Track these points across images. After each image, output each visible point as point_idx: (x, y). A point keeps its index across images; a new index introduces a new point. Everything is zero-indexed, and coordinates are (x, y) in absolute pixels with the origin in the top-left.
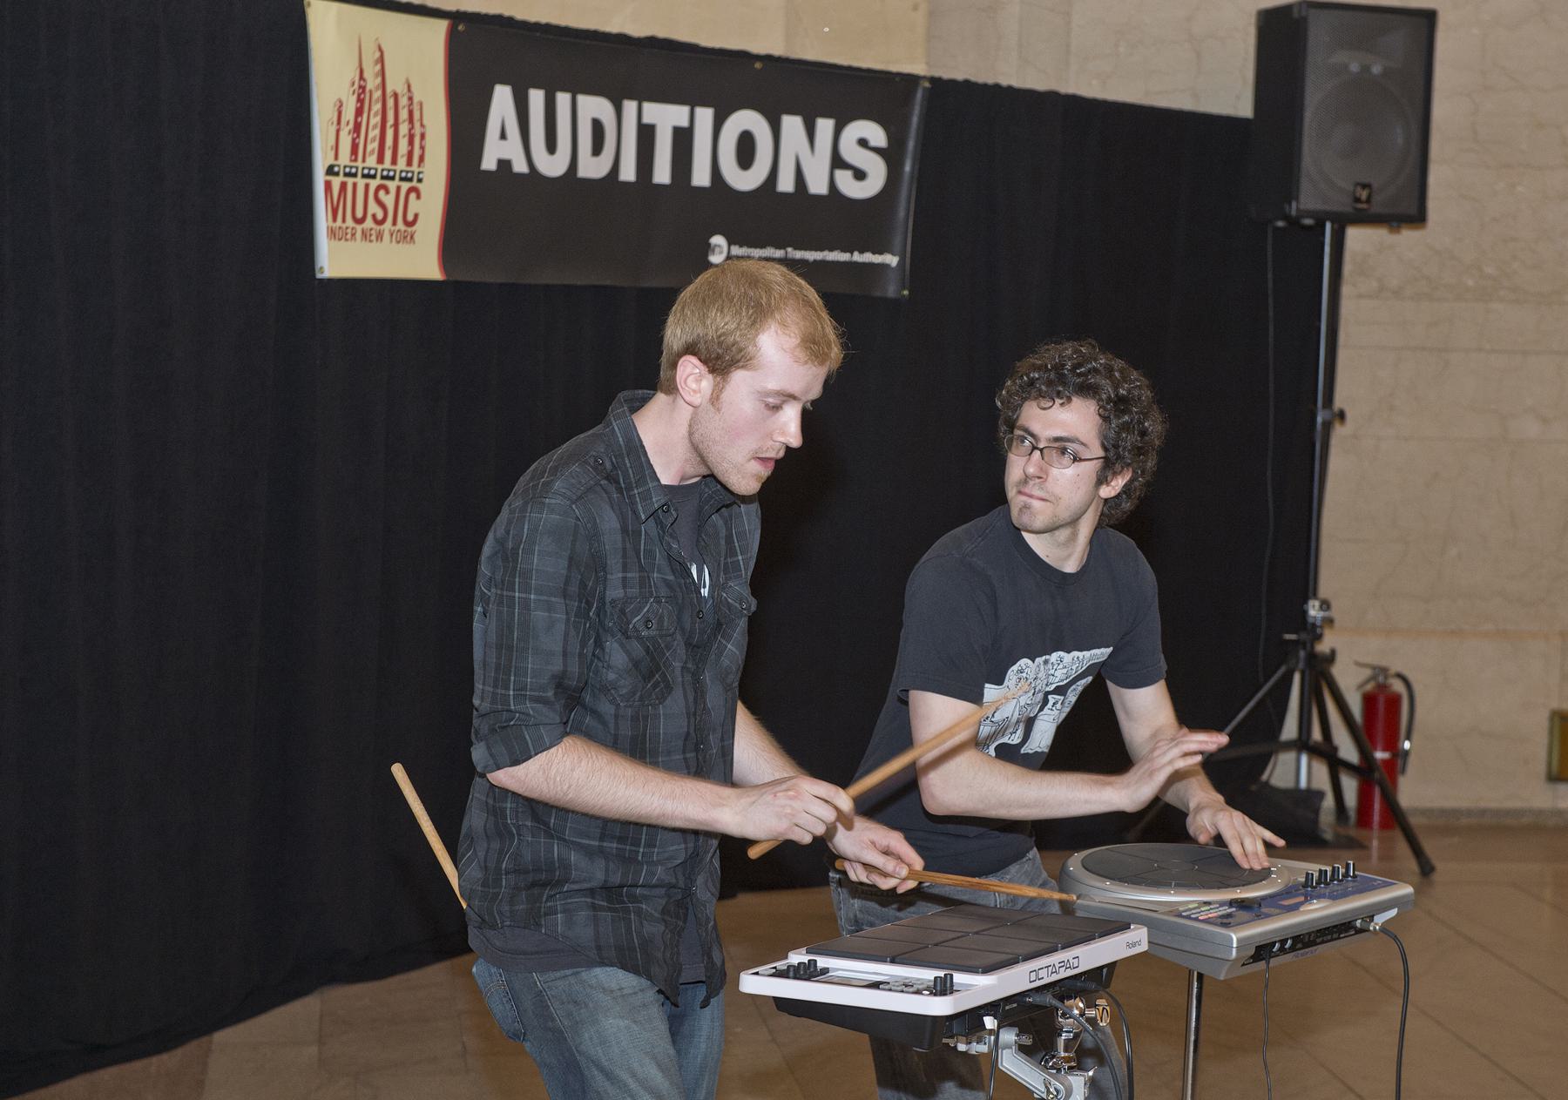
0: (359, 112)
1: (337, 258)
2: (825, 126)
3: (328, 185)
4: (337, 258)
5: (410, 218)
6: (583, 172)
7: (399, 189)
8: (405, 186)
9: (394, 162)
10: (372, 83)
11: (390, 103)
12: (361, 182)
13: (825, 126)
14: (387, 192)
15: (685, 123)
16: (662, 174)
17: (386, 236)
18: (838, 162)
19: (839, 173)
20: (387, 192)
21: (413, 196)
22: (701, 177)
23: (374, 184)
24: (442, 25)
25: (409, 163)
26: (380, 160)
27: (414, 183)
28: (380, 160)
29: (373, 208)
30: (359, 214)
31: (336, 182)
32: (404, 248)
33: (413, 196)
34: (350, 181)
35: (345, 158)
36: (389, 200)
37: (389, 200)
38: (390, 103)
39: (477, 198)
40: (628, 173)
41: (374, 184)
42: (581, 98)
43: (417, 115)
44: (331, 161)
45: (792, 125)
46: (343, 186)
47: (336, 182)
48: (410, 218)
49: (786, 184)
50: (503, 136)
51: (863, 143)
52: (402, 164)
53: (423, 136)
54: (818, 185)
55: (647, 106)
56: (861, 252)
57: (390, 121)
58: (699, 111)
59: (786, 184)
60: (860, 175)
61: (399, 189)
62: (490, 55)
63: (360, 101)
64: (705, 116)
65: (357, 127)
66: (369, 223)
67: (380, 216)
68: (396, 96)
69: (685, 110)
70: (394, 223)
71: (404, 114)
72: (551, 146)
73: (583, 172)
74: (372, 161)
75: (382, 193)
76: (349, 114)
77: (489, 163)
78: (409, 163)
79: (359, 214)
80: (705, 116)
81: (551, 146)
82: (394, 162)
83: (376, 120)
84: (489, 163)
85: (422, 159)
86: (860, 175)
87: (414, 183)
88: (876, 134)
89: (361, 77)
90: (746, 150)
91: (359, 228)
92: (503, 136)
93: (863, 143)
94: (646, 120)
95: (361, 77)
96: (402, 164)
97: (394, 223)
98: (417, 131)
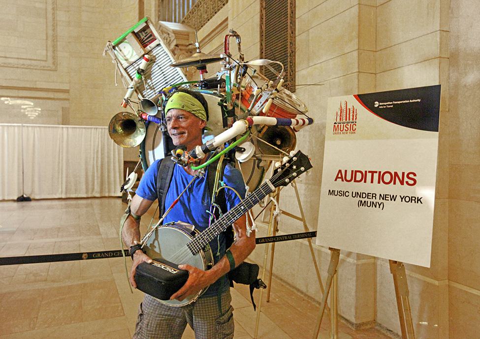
3: (335, 126)
7: (351, 125)
8: (352, 124)
9: (349, 120)
11: (348, 110)
21: (354, 125)
23: (345, 124)
26: (346, 120)
28: (346, 120)
29: (345, 128)
30: (342, 129)
33: (354, 125)
34: (340, 125)
36: (349, 127)
37: (349, 127)
38: (348, 110)
41: (345, 124)
43: (355, 111)
46: (338, 126)
48: (354, 129)
52: (351, 120)
61: (351, 125)
63: (341, 111)
65: (341, 116)
67: (347, 129)
68: (349, 109)
70: (350, 130)
71: (351, 112)
74: (344, 121)
76: (339, 114)
79: (342, 129)
85: (356, 119)
96: (351, 120)
97: (350, 130)
98: (355, 113)
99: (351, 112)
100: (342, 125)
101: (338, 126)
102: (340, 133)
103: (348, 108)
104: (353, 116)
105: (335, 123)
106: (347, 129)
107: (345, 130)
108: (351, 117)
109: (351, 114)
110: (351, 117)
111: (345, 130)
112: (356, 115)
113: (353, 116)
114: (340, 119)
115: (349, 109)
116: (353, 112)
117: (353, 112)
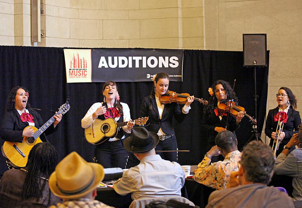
0: (74, 62)
1: (70, 80)
2: (167, 58)
3: (70, 71)
4: (70, 80)
5: (85, 74)
6: (120, 67)
8: (84, 71)
9: (81, 67)
10: (76, 58)
11: (80, 61)
12: (76, 71)
13: (167, 58)
14: (80, 71)
15: (141, 59)
16: (137, 66)
17: (81, 77)
18: (169, 62)
19: (170, 64)
20: (80, 71)
21: (85, 72)
22: (144, 66)
23: (78, 71)
24: (90, 50)
25: (84, 67)
26: (79, 67)
27: (85, 70)
28: (79, 67)
29: (78, 73)
30: (76, 74)
31: (71, 71)
32: (85, 78)
33: (85, 72)
34: (74, 71)
35: (73, 68)
38: (80, 61)
39: (95, 70)
40: (130, 66)
41: (78, 71)
42: (119, 57)
43: (85, 62)
44: (70, 68)
45: (161, 58)
46: (73, 71)
47: (71, 71)
48: (85, 74)
49: (160, 66)
50: (103, 63)
51: (174, 60)
52: (83, 68)
53: (86, 64)
54: (166, 66)
55: (133, 57)
56: (175, 75)
57: (80, 62)
58: (143, 57)
59: (160, 66)
60: (174, 64)
62: (97, 53)
64: (144, 58)
65: (74, 64)
66: (78, 76)
67: (80, 74)
68: (81, 60)
69: (141, 57)
70: (82, 75)
72: (113, 63)
73: (120, 67)
74: (77, 68)
75: (80, 72)
76: (73, 62)
77: (100, 66)
78: (84, 67)
79: (76, 74)
80: (144, 58)
81: (113, 63)
82: (81, 67)
83: (77, 63)
84: (100, 66)
85: (86, 67)
86: (174, 64)
87: (85, 70)
88: (176, 58)
89: (74, 58)
90: (152, 62)
91: (76, 76)
92: (103, 63)
93: (174, 60)
94: (133, 59)
95: (74, 58)
96: (83, 68)
97: (82, 75)
99: (82, 62)
100: (76, 71)
101: (73, 71)
102: (75, 77)
103: (80, 59)
104: (84, 65)
105: (70, 69)
106: (80, 74)
107: (79, 75)
108: (83, 66)
109: (83, 63)
110: (83, 66)
111: (79, 75)
112: (86, 64)
113: (84, 65)
114: (74, 67)
115: (81, 60)
116: (84, 62)
117: (84, 62)
